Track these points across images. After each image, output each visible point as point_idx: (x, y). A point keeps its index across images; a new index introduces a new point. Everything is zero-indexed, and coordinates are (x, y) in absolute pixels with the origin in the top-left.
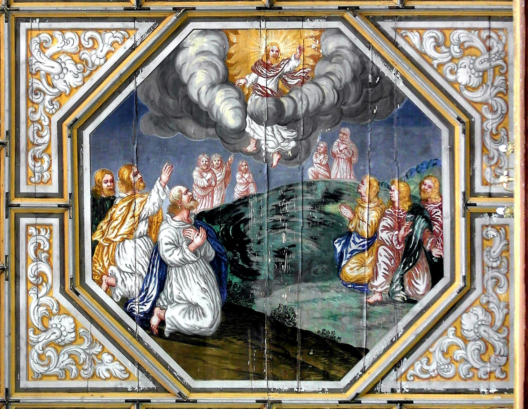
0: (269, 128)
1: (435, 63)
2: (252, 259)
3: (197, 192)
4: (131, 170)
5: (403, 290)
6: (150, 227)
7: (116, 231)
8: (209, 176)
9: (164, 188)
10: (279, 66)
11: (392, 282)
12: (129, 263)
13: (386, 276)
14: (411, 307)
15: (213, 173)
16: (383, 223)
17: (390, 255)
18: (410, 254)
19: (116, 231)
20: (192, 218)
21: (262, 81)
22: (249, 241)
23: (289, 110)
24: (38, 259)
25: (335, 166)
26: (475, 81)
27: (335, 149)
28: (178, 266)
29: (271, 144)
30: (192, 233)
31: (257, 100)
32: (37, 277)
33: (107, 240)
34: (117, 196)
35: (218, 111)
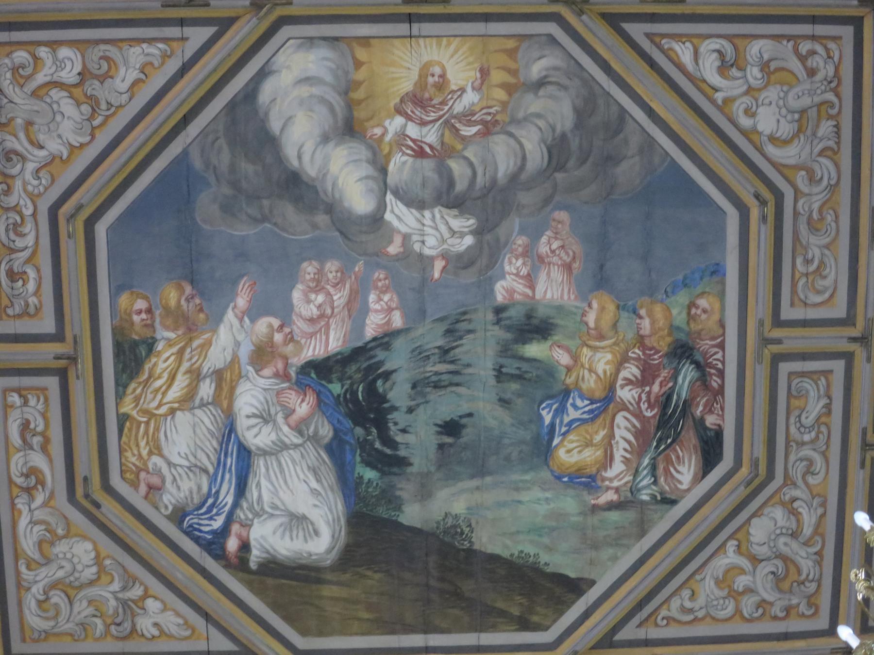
0: (427, 214)
1: (719, 97)
2: (399, 438)
3: (300, 326)
4: (181, 290)
5: (655, 482)
6: (219, 388)
7: (159, 396)
8: (320, 298)
9: (241, 320)
10: (443, 103)
11: (637, 471)
12: (184, 449)
13: (626, 461)
14: (667, 511)
15: (329, 294)
16: (624, 374)
17: (634, 426)
18: (668, 423)
19: (159, 396)
20: (293, 373)
21: (413, 131)
22: (394, 409)
23: (461, 186)
24: (27, 445)
25: (542, 277)
26: (786, 130)
27: (543, 249)
28: (273, 454)
29: (431, 241)
30: (292, 398)
31: (405, 163)
32: (27, 476)
33: (146, 412)
34: (158, 336)
35: (334, 184)
